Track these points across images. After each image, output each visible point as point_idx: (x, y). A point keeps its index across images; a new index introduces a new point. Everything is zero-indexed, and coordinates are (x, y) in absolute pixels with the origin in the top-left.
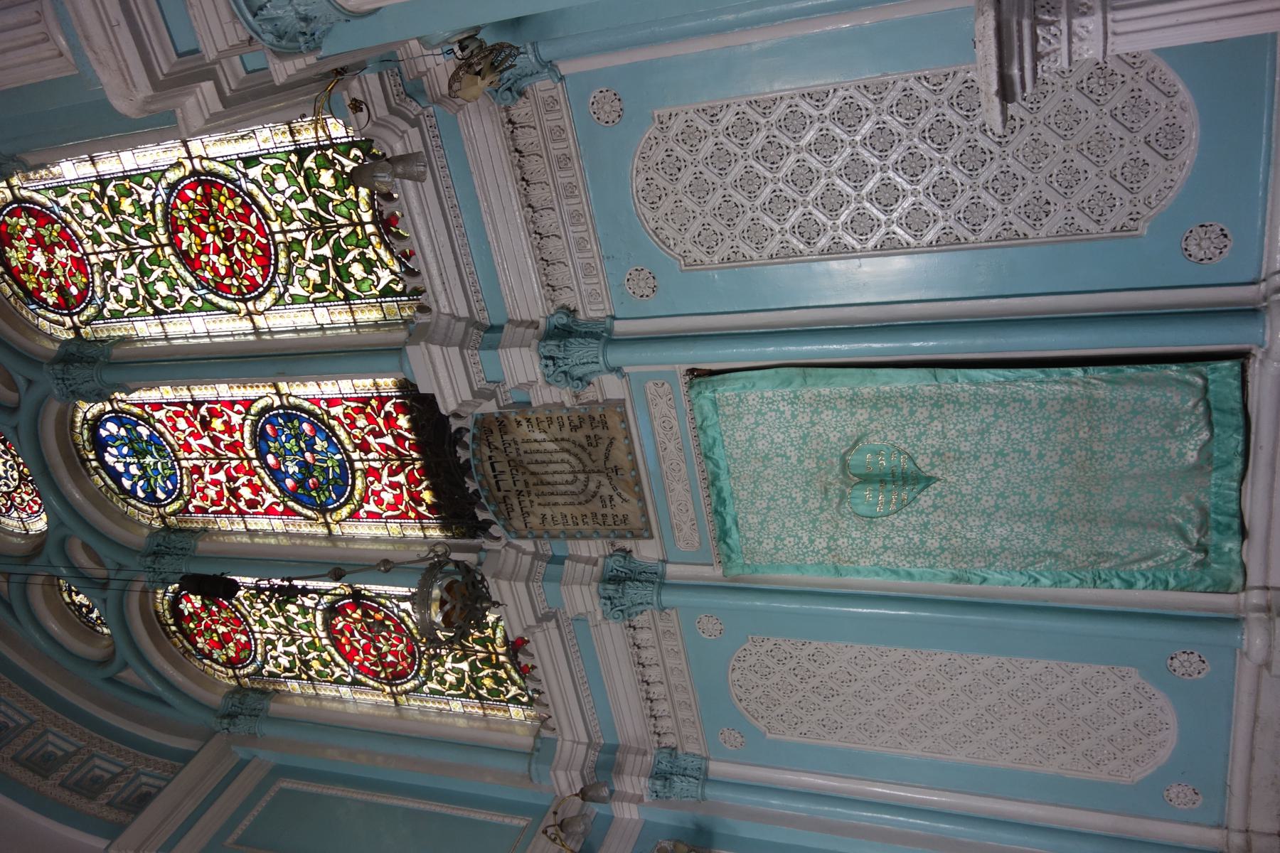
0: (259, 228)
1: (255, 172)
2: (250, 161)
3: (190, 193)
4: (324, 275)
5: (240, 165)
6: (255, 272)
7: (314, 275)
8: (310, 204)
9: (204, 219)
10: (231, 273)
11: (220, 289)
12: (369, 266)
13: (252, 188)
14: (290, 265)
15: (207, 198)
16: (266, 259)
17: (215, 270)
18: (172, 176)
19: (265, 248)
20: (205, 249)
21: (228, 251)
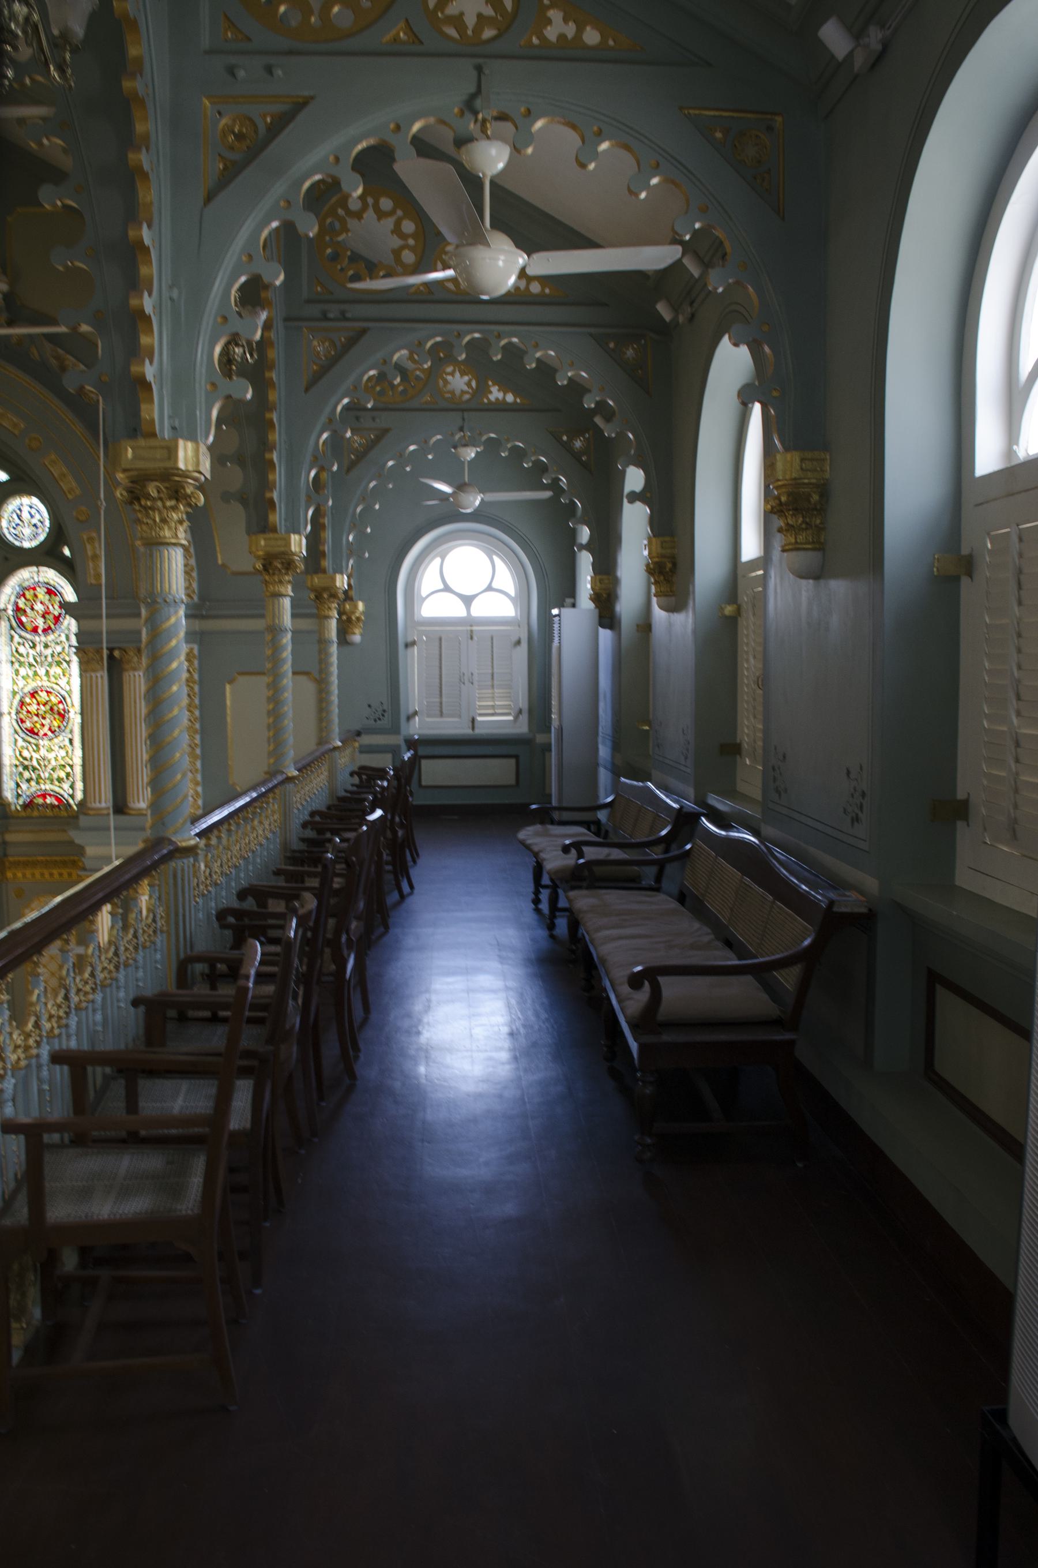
0: (45, 735)
1: (67, 742)
2: (71, 741)
3: (61, 706)
4: (25, 759)
5: (70, 736)
6: (28, 724)
7: (26, 754)
8: (53, 763)
9: (52, 709)
10: (28, 712)
11: (22, 703)
12: (28, 781)
13: (61, 738)
14: (30, 743)
15: (59, 714)
16: (32, 731)
17: (29, 704)
18: (68, 700)
19: (37, 734)
20: (38, 704)
21: (37, 715)
